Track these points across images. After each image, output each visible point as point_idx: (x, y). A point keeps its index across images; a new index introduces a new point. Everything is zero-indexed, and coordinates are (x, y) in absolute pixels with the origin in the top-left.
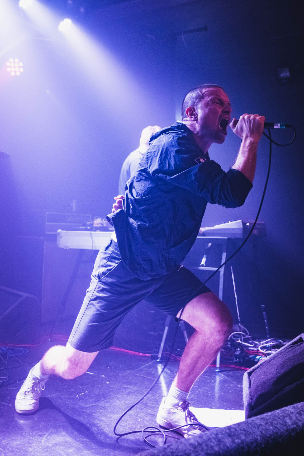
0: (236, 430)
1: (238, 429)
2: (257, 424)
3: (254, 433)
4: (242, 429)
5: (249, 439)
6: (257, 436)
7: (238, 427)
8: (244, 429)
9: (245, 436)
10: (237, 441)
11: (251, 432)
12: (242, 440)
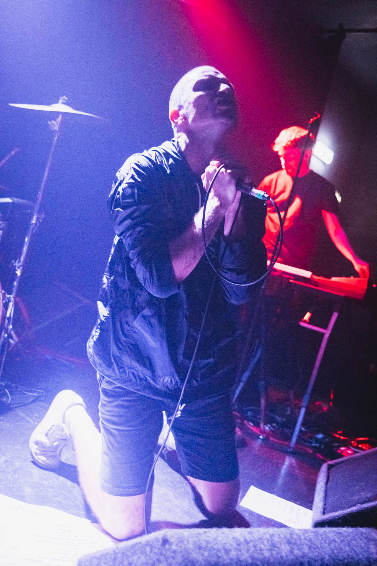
0: (299, 537)
1: (302, 537)
2: (330, 538)
3: (323, 549)
4: (308, 538)
5: (313, 555)
6: (325, 554)
7: (304, 534)
8: (310, 539)
9: (310, 548)
10: (296, 552)
11: (319, 546)
12: (304, 553)
